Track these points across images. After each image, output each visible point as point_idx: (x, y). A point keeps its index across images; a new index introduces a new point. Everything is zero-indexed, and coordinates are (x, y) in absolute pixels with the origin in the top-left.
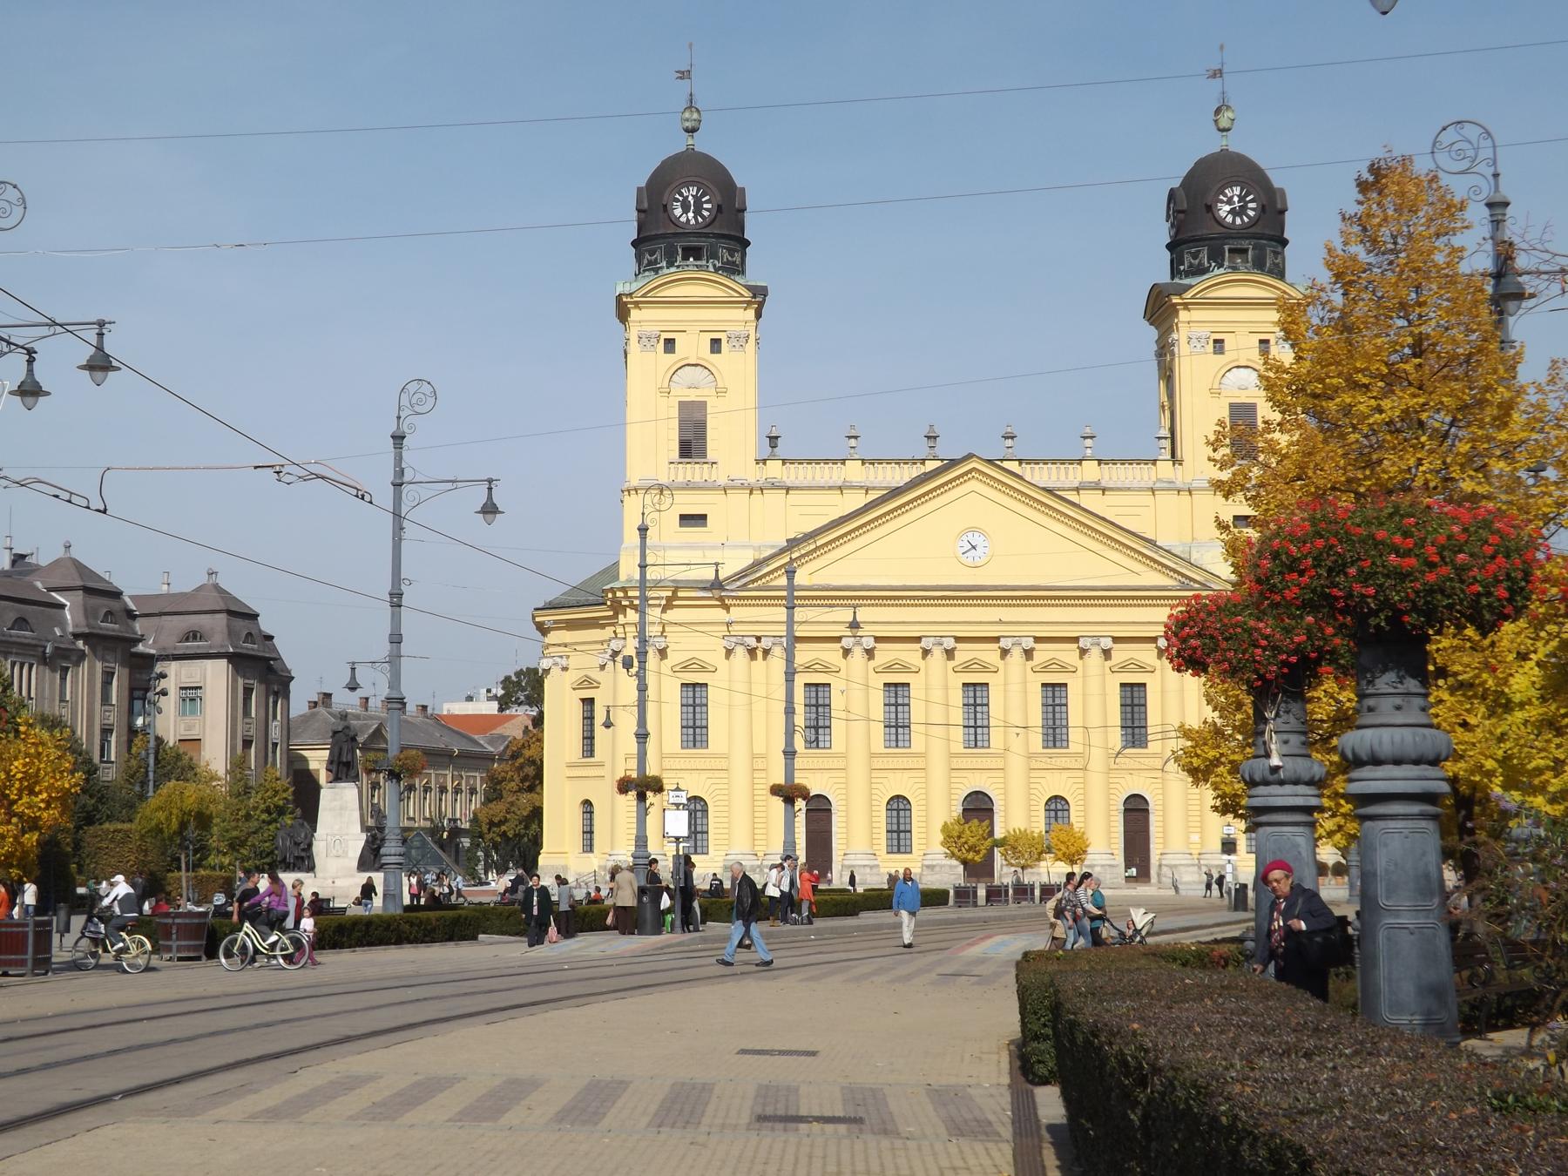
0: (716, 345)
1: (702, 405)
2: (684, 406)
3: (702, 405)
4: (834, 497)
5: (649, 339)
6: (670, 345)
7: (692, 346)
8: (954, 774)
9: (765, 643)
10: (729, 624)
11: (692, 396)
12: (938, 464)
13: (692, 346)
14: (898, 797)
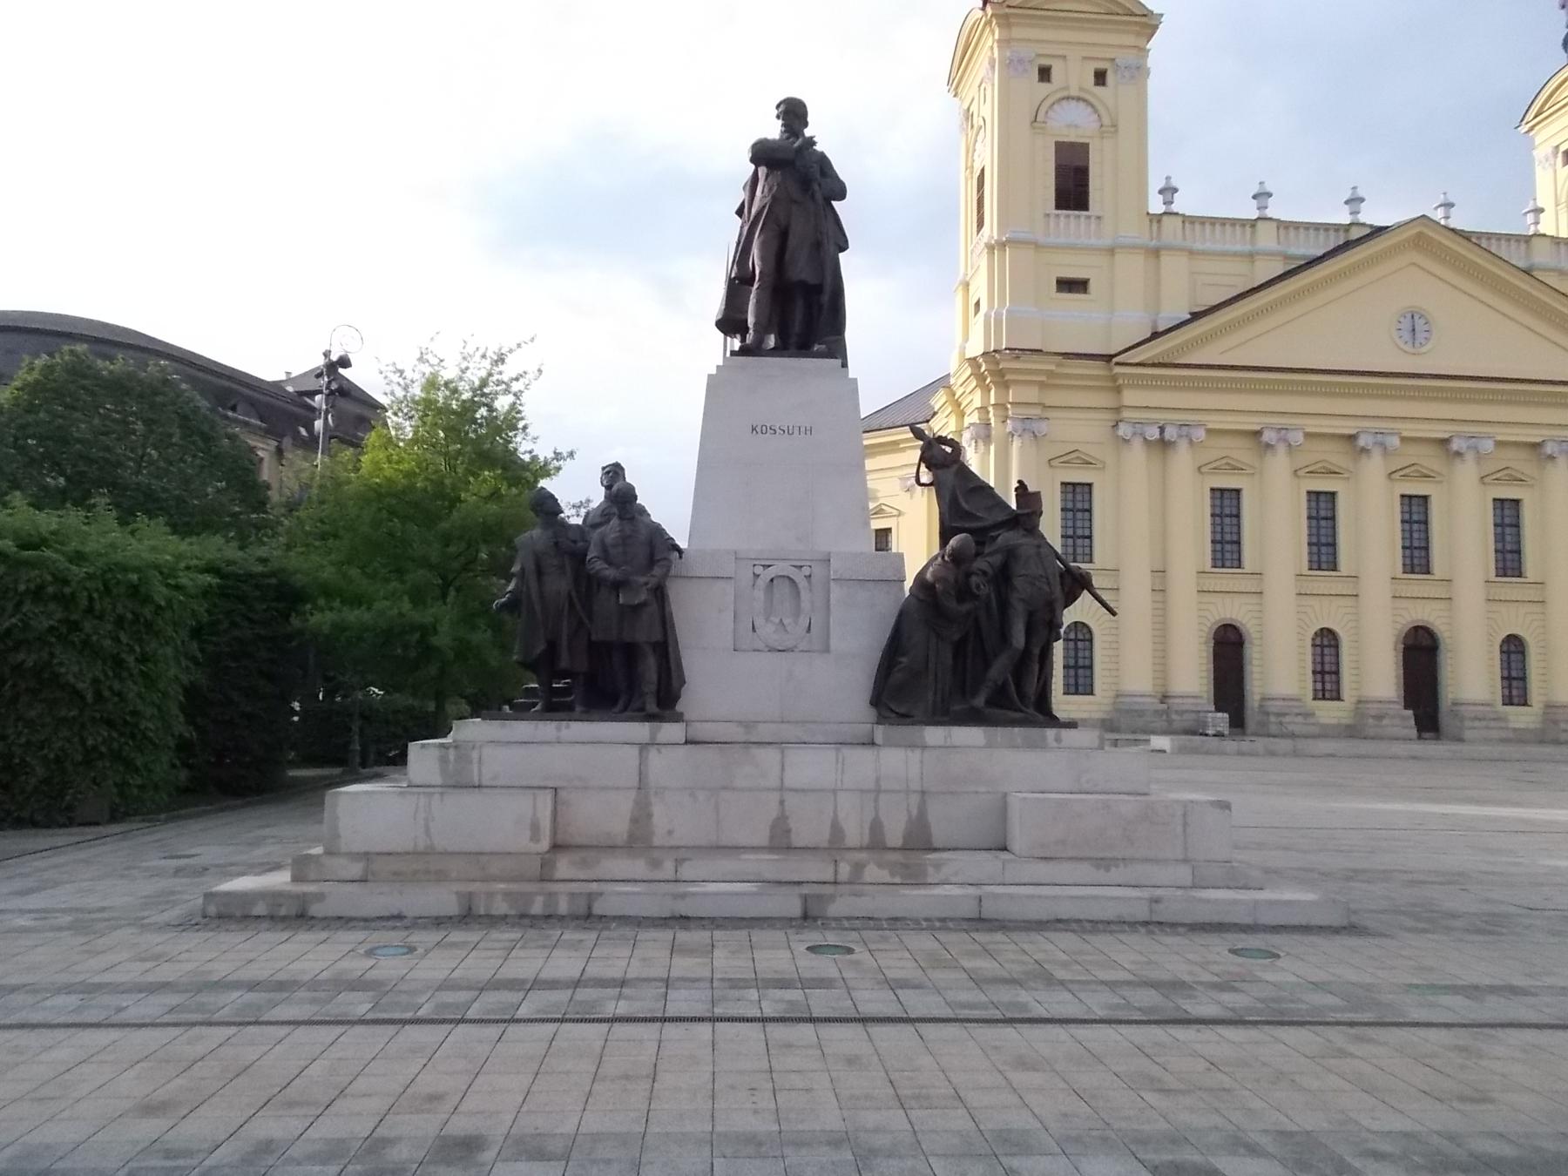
0: (1100, 78)
1: (1083, 149)
2: (1062, 149)
3: (1083, 149)
4: (1241, 267)
5: (1020, 61)
6: (1045, 74)
7: (1073, 74)
8: (1399, 603)
9: (1171, 433)
10: (1118, 410)
11: (1072, 137)
12: (1368, 231)
13: (1073, 74)
14: (1330, 631)
